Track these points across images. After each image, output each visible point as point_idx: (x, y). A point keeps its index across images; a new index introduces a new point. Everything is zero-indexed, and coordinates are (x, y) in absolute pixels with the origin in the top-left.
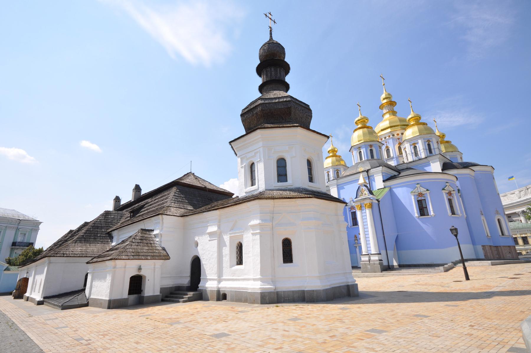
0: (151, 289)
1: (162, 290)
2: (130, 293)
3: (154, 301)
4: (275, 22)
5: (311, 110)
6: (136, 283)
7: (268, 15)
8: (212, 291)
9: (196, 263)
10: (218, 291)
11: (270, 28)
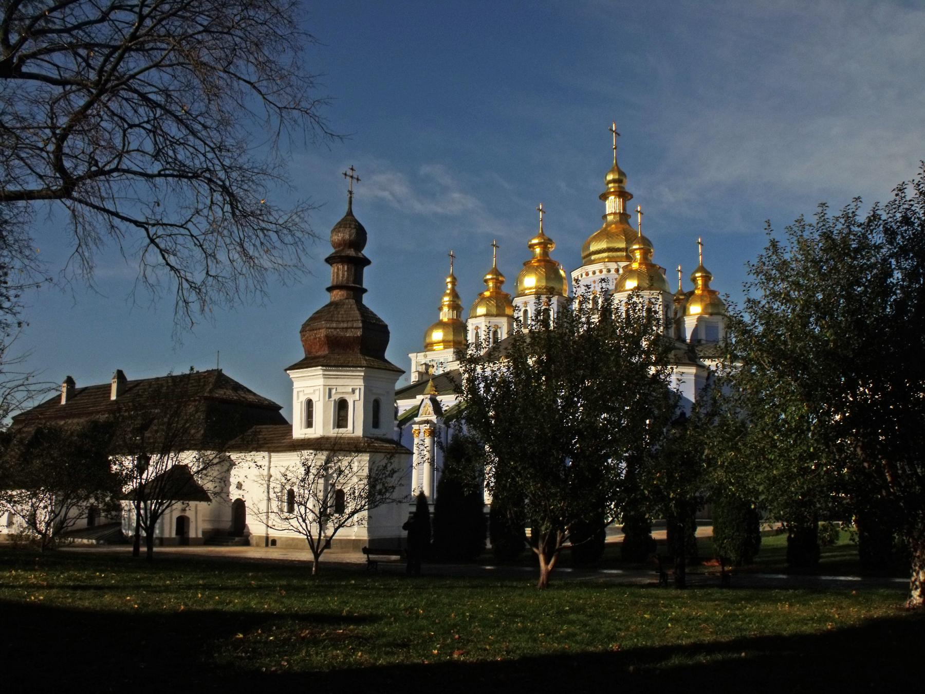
0: (194, 532)
1: (204, 533)
2: (177, 534)
3: (197, 542)
4: (358, 179)
5: (388, 333)
6: (182, 523)
7: (350, 173)
8: (260, 537)
9: (239, 507)
10: (267, 538)
11: (351, 192)
